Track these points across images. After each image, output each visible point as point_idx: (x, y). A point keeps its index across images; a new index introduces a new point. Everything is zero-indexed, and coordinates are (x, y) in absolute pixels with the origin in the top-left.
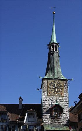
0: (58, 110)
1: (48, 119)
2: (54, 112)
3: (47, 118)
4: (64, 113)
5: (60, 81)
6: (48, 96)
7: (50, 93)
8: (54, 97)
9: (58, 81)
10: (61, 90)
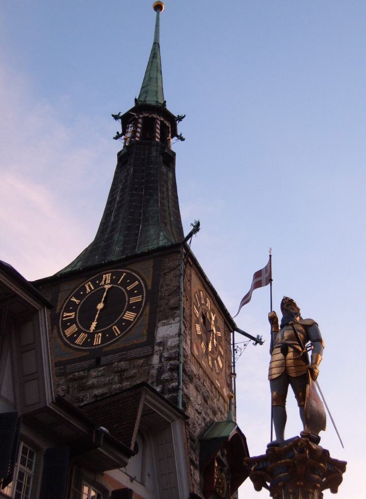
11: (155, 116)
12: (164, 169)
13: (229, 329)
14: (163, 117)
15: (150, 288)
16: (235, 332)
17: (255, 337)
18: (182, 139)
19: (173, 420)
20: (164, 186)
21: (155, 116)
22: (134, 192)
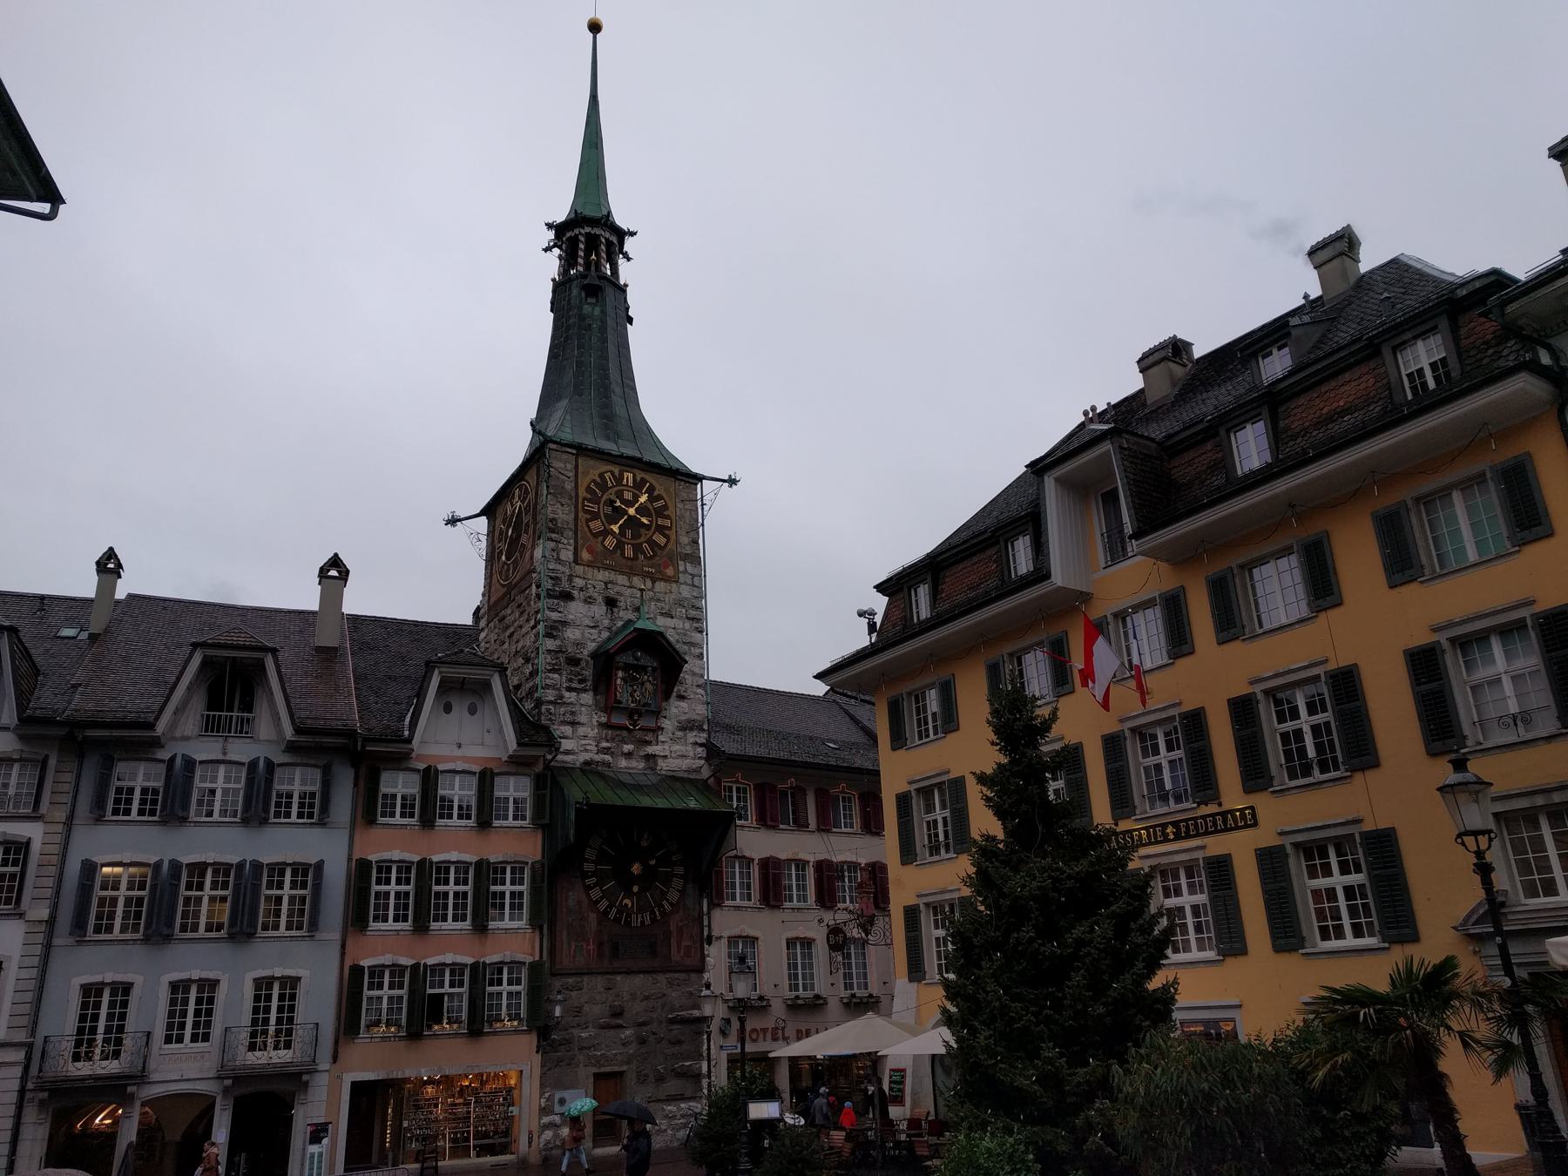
0: (644, 669)
1: (581, 731)
2: (619, 681)
3: (573, 724)
4: (681, 697)
5: (651, 478)
6: (579, 569)
7: (590, 551)
8: (622, 579)
10: (661, 540)
11: (576, 231)
13: (692, 483)
17: (727, 478)
18: (632, 234)
19: (492, 676)
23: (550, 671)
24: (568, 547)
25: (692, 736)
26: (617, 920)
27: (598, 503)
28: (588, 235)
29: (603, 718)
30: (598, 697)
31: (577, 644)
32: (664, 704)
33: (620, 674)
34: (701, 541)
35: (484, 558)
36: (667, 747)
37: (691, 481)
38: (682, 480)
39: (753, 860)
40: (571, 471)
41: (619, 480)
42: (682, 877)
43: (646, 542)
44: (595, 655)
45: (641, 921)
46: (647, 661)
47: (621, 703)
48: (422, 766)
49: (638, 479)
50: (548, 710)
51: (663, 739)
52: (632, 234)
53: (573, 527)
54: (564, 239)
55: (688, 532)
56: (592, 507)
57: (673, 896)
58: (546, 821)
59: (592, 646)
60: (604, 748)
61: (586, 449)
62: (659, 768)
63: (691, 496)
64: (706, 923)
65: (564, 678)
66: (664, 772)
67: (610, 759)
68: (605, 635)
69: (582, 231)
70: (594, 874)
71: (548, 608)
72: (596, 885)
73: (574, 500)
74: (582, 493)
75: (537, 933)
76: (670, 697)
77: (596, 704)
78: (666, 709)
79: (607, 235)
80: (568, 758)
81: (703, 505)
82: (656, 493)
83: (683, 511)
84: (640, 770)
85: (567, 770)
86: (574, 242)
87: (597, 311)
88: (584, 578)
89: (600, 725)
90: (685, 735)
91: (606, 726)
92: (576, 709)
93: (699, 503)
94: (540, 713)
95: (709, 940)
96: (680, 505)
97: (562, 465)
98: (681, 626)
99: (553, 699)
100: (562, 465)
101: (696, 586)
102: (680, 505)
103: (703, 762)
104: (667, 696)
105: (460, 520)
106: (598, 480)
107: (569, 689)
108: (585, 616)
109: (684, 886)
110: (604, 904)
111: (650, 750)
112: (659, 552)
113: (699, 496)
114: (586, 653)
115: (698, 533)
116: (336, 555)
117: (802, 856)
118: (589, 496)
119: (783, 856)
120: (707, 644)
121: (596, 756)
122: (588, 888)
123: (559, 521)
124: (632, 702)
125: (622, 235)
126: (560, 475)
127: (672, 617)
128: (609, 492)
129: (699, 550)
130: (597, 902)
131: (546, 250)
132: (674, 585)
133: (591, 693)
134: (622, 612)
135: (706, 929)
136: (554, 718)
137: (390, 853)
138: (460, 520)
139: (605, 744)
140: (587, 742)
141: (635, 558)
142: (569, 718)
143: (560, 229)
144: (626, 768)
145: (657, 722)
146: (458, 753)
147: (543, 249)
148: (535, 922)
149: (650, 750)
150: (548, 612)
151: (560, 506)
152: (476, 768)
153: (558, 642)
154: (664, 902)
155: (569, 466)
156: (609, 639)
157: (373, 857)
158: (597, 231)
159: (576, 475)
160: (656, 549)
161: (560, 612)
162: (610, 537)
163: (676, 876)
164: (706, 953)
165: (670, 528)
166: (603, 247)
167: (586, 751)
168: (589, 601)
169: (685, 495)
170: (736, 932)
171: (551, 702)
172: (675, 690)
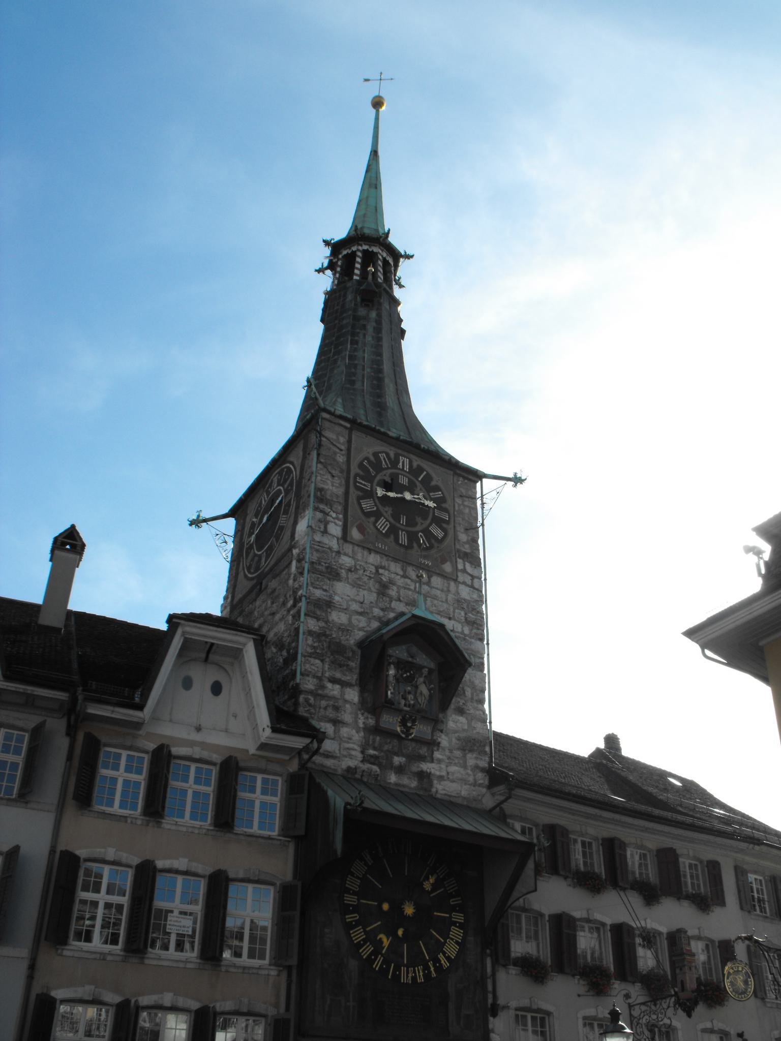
0: (421, 668)
1: (345, 731)
3: (336, 722)
4: (461, 711)
5: (426, 465)
6: (348, 548)
7: (361, 529)
8: (395, 567)
9: (417, 462)
10: (439, 534)
11: (354, 249)
12: (362, 312)
14: (365, 244)
15: (298, 477)
16: (484, 480)
17: (511, 476)
18: (408, 257)
19: (245, 645)
20: (359, 333)
21: (354, 249)
22: (323, 358)
23: (311, 655)
24: (336, 521)
25: (471, 760)
26: (384, 972)
27: (371, 482)
28: (365, 252)
29: (370, 720)
30: (366, 695)
31: (346, 630)
32: (441, 715)
33: (392, 672)
34: (480, 542)
35: (229, 559)
36: (443, 766)
37: (471, 477)
38: (460, 475)
39: (542, 915)
40: (343, 444)
41: (395, 463)
42: (461, 926)
43: (422, 531)
44: (361, 644)
45: (412, 977)
46: (422, 659)
47: (393, 704)
48: (152, 746)
49: (415, 465)
50: (307, 700)
51: (440, 757)
52: (408, 257)
53: (341, 500)
54: (340, 256)
55: (467, 529)
56: (364, 485)
57: (451, 949)
58: (302, 832)
59: (360, 635)
60: (371, 756)
61: (360, 424)
62: (434, 790)
63: (470, 493)
64: (490, 988)
65: (327, 666)
66: (439, 796)
67: (378, 770)
68: (375, 625)
69: (360, 248)
70: (356, 909)
71: (312, 584)
72: (358, 923)
73: (345, 474)
74: (354, 469)
75: (284, 975)
76: (447, 708)
77: (363, 702)
78: (442, 722)
79: (385, 255)
80: (329, 763)
81: (483, 504)
82: (433, 483)
83: (462, 507)
84: (410, 788)
85: (329, 774)
86: (350, 259)
87: (373, 314)
88: (353, 558)
89: (368, 730)
90: (465, 756)
91: (377, 730)
92: (340, 703)
93: (479, 502)
94: (296, 704)
95: (494, 1010)
96: (458, 501)
97: (334, 437)
98: (460, 630)
99: (312, 687)
100: (334, 437)
101: (474, 588)
102: (458, 501)
103: (484, 790)
104: (444, 706)
105: (205, 521)
106: (372, 458)
107: (333, 681)
108: (354, 600)
109: (464, 938)
110: (367, 951)
111: (425, 766)
112: (436, 545)
113: (479, 495)
114: (352, 642)
115: (478, 532)
116: (73, 527)
117: (598, 916)
118: (361, 473)
119: (577, 914)
120: (488, 655)
121: (361, 765)
122: (349, 926)
123: (329, 493)
124: (405, 705)
125: (396, 256)
126: (331, 446)
127: (450, 619)
128: (384, 472)
129: (479, 550)
130: (359, 946)
131: (319, 271)
132: (452, 584)
133: (357, 688)
134: (394, 602)
135: (490, 996)
136: (312, 711)
137: (103, 850)
138: (205, 521)
139: (371, 752)
140: (351, 745)
141: (409, 547)
142: (331, 713)
143: (336, 247)
144: (396, 784)
145: (432, 735)
146: (195, 736)
147: (316, 271)
148: (277, 961)
149: (425, 766)
150: (311, 588)
151: (329, 477)
152: (217, 758)
153: (322, 624)
154: (441, 956)
155: (342, 439)
156: (379, 629)
157: (82, 853)
158: (376, 249)
159: (349, 450)
160: (433, 541)
161: (325, 590)
162: (383, 520)
163: (454, 924)
164: (491, 1026)
165: (448, 522)
166: (380, 263)
167: (351, 757)
168: (356, 585)
169: (463, 491)
170: (525, 1002)
171: (311, 692)
172: (454, 700)
